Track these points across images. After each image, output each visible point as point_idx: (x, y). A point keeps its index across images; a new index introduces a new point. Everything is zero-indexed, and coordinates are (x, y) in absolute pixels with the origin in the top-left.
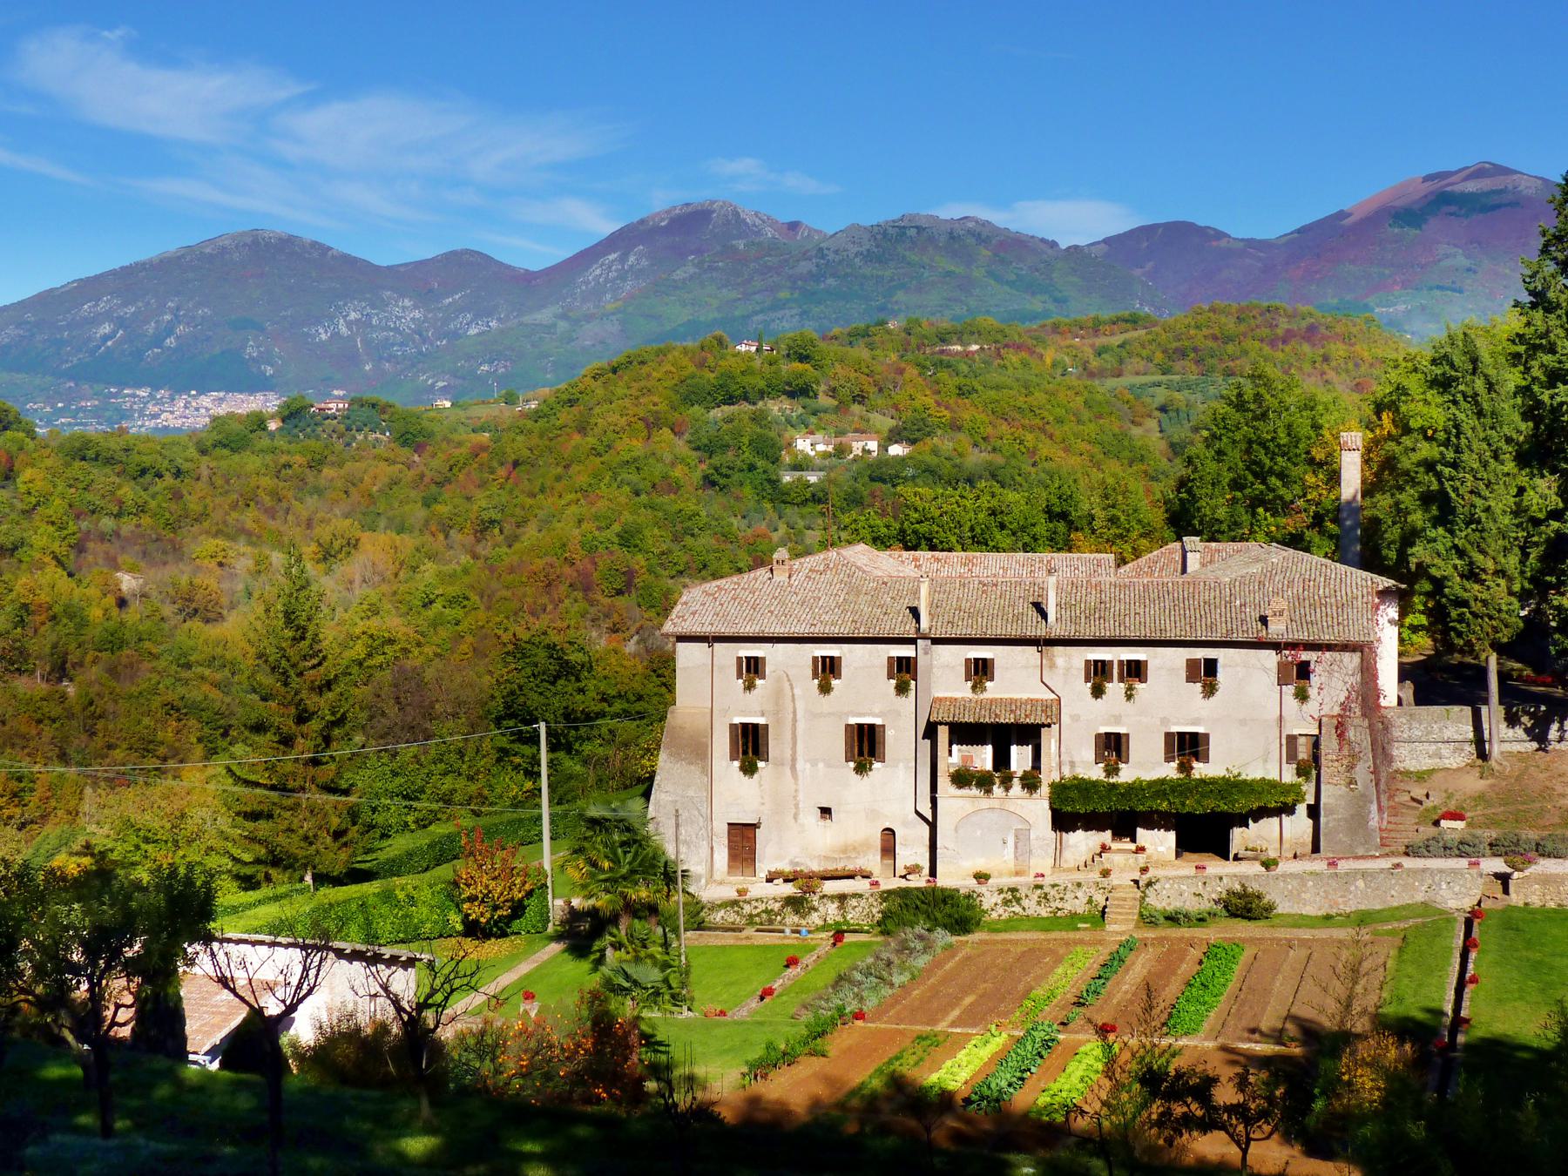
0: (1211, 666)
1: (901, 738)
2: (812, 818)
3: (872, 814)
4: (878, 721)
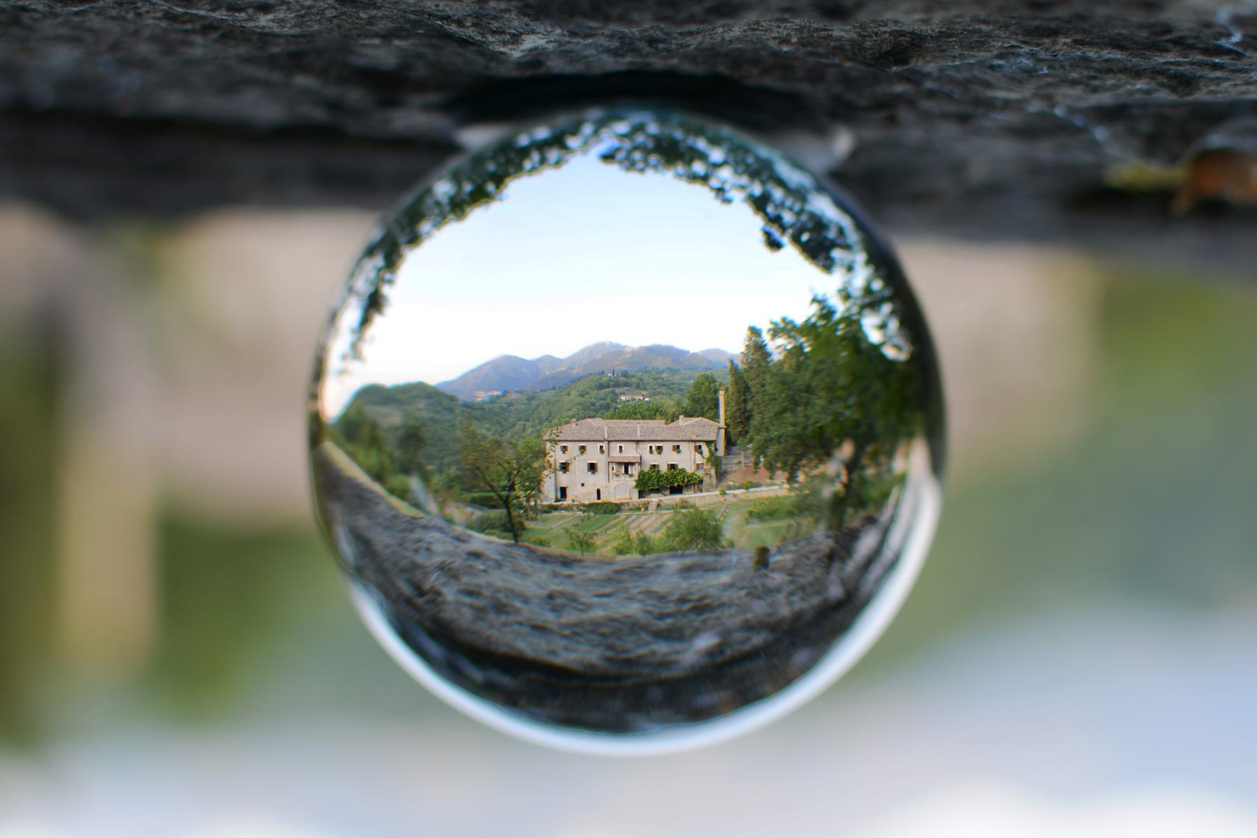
0: (678, 447)
1: (601, 467)
2: (580, 485)
3: (594, 485)
4: (595, 462)
